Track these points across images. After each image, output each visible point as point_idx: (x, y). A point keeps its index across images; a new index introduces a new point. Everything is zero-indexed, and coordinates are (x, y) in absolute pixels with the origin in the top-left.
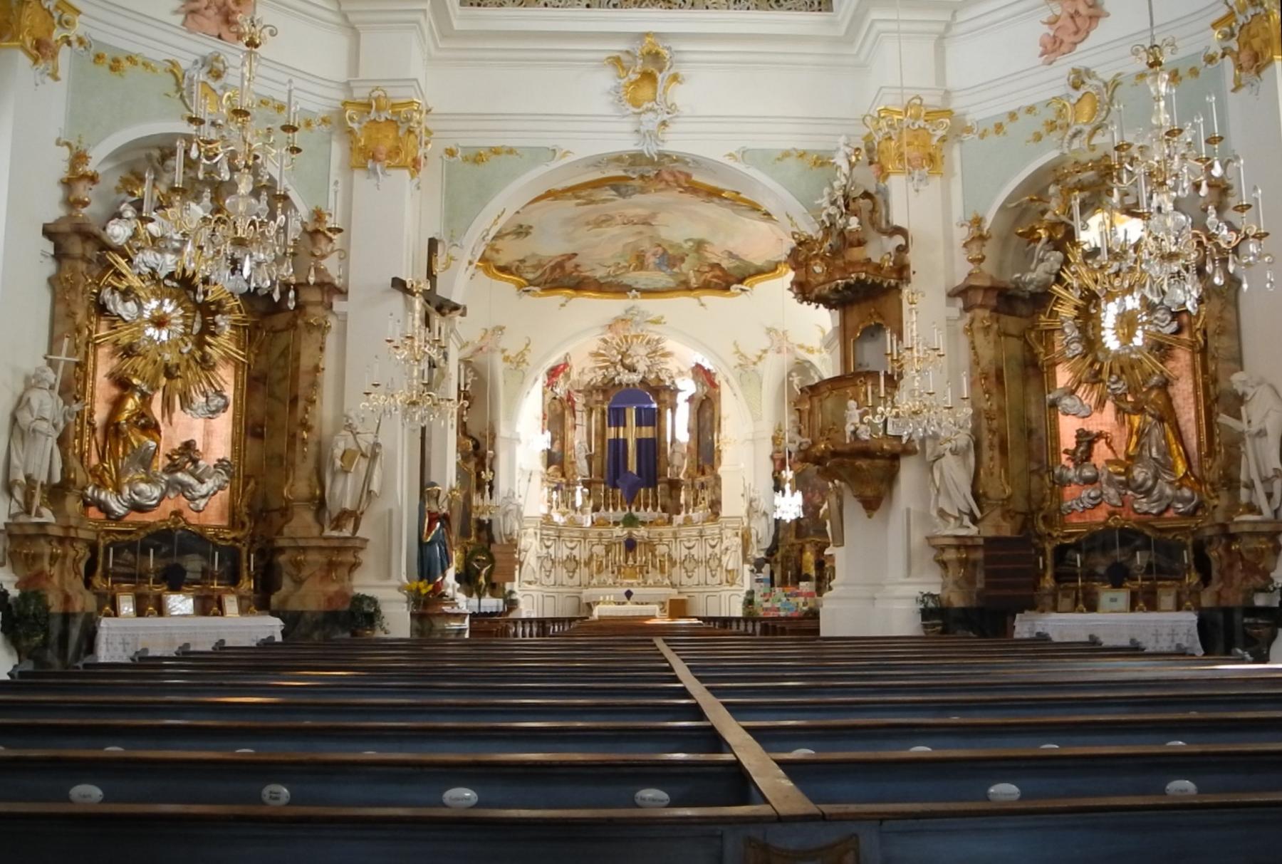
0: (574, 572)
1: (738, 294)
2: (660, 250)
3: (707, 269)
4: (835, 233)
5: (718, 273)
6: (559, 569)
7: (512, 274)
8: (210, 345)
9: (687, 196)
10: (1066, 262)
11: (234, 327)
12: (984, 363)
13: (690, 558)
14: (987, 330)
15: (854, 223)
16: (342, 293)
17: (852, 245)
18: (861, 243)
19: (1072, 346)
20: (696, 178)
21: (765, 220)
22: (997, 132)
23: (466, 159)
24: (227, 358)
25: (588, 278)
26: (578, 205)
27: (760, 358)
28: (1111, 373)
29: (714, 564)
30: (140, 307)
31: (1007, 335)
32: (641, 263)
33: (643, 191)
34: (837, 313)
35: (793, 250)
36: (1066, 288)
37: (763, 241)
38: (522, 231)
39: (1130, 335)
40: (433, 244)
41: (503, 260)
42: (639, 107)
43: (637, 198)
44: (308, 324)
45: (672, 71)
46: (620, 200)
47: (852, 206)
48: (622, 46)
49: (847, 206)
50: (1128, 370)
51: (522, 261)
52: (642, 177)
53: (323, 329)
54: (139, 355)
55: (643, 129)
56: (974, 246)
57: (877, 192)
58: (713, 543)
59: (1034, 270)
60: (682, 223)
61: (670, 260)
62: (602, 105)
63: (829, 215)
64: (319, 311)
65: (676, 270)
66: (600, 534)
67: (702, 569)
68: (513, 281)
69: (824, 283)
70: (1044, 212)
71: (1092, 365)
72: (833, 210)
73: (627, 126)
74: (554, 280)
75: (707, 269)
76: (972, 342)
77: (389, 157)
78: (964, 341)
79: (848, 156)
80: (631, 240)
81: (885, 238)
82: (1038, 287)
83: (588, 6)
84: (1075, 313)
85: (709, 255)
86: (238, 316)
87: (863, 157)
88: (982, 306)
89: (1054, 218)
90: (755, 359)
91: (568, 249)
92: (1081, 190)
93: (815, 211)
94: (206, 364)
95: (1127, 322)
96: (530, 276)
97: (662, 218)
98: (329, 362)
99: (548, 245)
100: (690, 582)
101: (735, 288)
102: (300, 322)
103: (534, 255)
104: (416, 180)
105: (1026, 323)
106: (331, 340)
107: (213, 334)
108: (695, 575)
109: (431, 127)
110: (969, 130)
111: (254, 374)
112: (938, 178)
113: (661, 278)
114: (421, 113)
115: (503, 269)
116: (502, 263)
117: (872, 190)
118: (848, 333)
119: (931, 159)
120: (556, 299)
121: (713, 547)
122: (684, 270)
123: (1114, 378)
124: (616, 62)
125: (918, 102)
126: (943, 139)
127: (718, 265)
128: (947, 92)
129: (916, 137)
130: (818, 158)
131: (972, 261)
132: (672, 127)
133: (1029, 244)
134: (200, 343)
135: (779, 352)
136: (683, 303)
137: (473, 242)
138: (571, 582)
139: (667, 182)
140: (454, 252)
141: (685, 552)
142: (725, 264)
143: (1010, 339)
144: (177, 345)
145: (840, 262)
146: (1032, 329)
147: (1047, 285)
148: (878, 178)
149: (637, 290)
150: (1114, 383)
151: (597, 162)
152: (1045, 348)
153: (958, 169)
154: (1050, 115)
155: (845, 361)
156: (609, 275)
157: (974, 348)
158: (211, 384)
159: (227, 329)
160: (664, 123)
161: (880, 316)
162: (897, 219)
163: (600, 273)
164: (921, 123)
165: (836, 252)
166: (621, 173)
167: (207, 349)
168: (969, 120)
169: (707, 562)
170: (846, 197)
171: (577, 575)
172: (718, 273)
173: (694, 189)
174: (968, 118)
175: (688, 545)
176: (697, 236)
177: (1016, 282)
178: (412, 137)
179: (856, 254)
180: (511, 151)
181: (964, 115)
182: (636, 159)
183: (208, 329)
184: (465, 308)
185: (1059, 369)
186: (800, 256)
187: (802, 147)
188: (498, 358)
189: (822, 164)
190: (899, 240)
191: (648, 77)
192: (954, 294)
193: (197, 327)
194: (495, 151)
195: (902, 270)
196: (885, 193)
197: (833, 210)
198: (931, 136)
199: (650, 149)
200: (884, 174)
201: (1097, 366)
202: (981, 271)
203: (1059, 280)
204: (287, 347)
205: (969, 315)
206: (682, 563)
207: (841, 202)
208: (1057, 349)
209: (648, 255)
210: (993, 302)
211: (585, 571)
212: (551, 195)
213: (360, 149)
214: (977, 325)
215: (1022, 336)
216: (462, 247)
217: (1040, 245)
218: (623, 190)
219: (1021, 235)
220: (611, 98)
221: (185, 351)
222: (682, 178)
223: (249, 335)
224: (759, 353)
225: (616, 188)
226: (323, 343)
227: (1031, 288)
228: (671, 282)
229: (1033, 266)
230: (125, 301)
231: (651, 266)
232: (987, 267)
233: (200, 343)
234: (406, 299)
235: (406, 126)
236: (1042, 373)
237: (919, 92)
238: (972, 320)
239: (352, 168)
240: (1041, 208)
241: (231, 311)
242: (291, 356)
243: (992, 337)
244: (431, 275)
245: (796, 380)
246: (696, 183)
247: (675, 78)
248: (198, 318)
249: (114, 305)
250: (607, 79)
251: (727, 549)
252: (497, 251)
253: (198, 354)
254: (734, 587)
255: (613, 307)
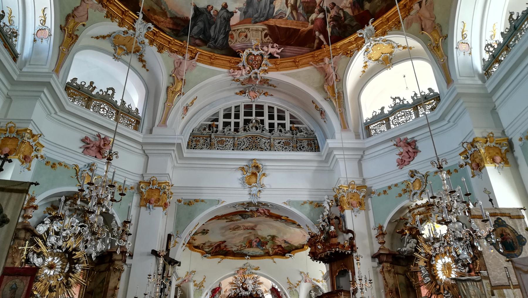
1: (288, 258)
2: (258, 240)
3: (276, 247)
4: (325, 233)
5: (280, 249)
7: (200, 249)
8: (71, 277)
9: (268, 218)
10: (418, 243)
11: (83, 269)
12: (390, 286)
14: (389, 271)
15: (332, 228)
16: (131, 256)
17: (332, 237)
18: (336, 236)
19: (426, 278)
20: (272, 211)
21: (298, 228)
22: (384, 194)
23: (185, 204)
24: (78, 283)
25: (229, 251)
26: (227, 222)
27: (298, 285)
28: (444, 290)
30: (44, 260)
31: (398, 274)
32: (250, 245)
33: (252, 216)
34: (328, 265)
35: (309, 239)
36: (420, 254)
37: (297, 236)
38: (205, 232)
39: (450, 273)
40: (169, 236)
41: (197, 243)
42: (250, 185)
43: (249, 219)
44: (114, 268)
45: (263, 172)
46: (243, 220)
47: (331, 222)
48: (245, 164)
49: (329, 222)
50: (451, 288)
51: (204, 244)
52: (251, 211)
53: (121, 271)
54: (39, 281)
55: (252, 193)
56: (380, 237)
57: (341, 216)
59: (406, 247)
60: (267, 229)
61: (262, 243)
62: (237, 184)
63: (322, 226)
64: (120, 263)
65: (264, 248)
68: (200, 252)
69: (322, 253)
70: (406, 223)
71: (435, 286)
72: (324, 224)
73: (246, 191)
74: (217, 252)
75: (276, 247)
76: (384, 277)
77: (155, 202)
78: (380, 276)
79: (328, 203)
80: (247, 235)
81: (345, 234)
82: (408, 253)
83: (233, 150)
84: (425, 264)
85: (277, 242)
86: (85, 265)
87: (334, 203)
88: (386, 262)
89: (410, 226)
90: (296, 285)
91: (222, 239)
92: (420, 215)
93: (317, 224)
94: (68, 286)
95: (447, 267)
96: (207, 250)
97: (258, 227)
98: (121, 285)
99: (214, 237)
101: (287, 255)
102: (111, 268)
103: (209, 241)
104: (165, 211)
105: (405, 268)
106: (124, 276)
107: (73, 273)
109: (172, 192)
110: (374, 193)
111: (88, 290)
112: (363, 211)
113: (258, 251)
114: (169, 186)
115: (197, 247)
116: (196, 245)
117: (339, 216)
118: (333, 273)
119: (360, 204)
120: (217, 259)
122: (267, 248)
123: (446, 292)
124: (242, 169)
125: (353, 183)
126: (364, 196)
127: (280, 246)
128: (364, 179)
129: (354, 196)
130: (317, 204)
131: (380, 243)
132: (263, 193)
133: (402, 236)
134: (67, 276)
135: (306, 281)
136: (267, 261)
137: (185, 236)
139: (261, 213)
140: (178, 240)
142: (283, 245)
143: (400, 276)
144: (57, 277)
145: (328, 244)
146: (408, 271)
147: (412, 253)
148: (340, 211)
149: (249, 256)
150: (446, 294)
151: (234, 205)
152: (415, 279)
153: (371, 207)
154: (404, 187)
155: (333, 285)
156: (238, 250)
157: (385, 279)
158: (69, 295)
159: (80, 270)
160: (260, 191)
161: (346, 266)
162: (349, 227)
163: (235, 249)
164: (355, 191)
165: (326, 240)
166: (243, 210)
167: (70, 279)
168: (373, 189)
170: (328, 218)
172: (280, 249)
173: (271, 216)
174: (373, 188)
176: (272, 234)
177: (399, 251)
178: (165, 195)
179: (334, 241)
180: (202, 201)
181: (371, 187)
182: (250, 204)
183: (72, 270)
184: (180, 263)
185: (422, 288)
186: (312, 242)
187: (311, 200)
188: (191, 285)
189: (319, 206)
190: (350, 235)
191: (254, 174)
192: (374, 257)
193: (67, 269)
194: (196, 201)
195: (352, 246)
196: (343, 217)
197: (324, 224)
198: (359, 195)
199: (255, 200)
200: (342, 210)
201: (438, 287)
202: (384, 247)
203: (417, 251)
204: (105, 278)
205: (381, 265)
207: (327, 220)
208: (420, 279)
209: (253, 241)
210: (391, 260)
212: (218, 218)
213: (144, 199)
214: (385, 270)
215: (404, 274)
216: (181, 238)
217: (406, 237)
218: (244, 216)
219: (398, 232)
220: (240, 182)
221: (59, 280)
222: (266, 211)
223: (88, 273)
224: (298, 283)
225: (241, 215)
226: (120, 277)
227: (406, 253)
228: (262, 252)
229: (405, 245)
230: (38, 258)
231: (255, 246)
232: (386, 245)
233: (67, 276)
234: (156, 258)
235: (163, 191)
236: (415, 290)
237: (354, 179)
238: (383, 267)
239: (140, 206)
240: (405, 222)
241: (83, 263)
242: (105, 282)
243: (392, 275)
244: (168, 249)
245: (313, 294)
246: (271, 213)
247: (264, 174)
248: (68, 266)
249: (33, 259)
250: (239, 175)
252: (195, 240)
253: (65, 282)
255: (239, 263)
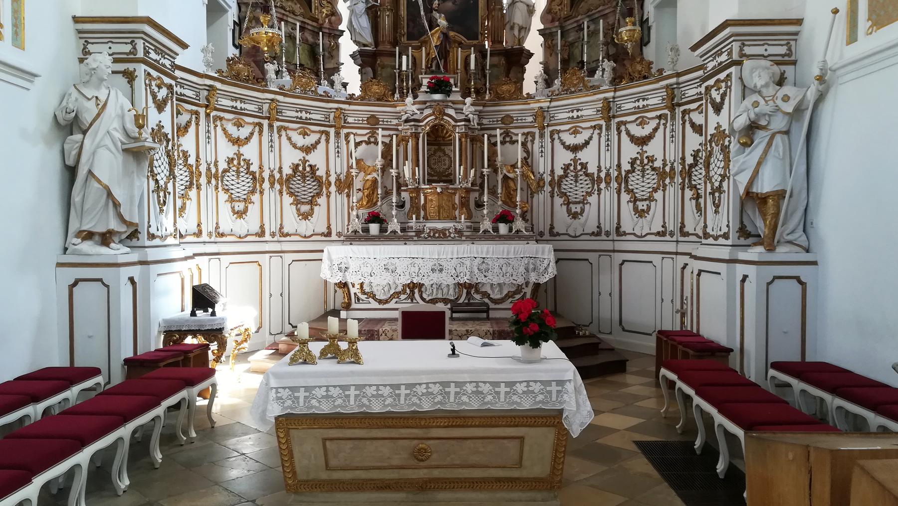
0: (312, 203)
6: (270, 196)
13: (577, 169)
29: (641, 184)
58: (639, 132)
66: (373, 122)
67: (608, 196)
100: (576, 227)
108: (591, 211)
121: (642, 141)
138: (305, 227)
141: (564, 157)
169: (623, 180)
171: (320, 212)
175: (570, 140)
206: (556, 183)
211: (338, 200)
251: (753, 127)
254: (783, 252)
